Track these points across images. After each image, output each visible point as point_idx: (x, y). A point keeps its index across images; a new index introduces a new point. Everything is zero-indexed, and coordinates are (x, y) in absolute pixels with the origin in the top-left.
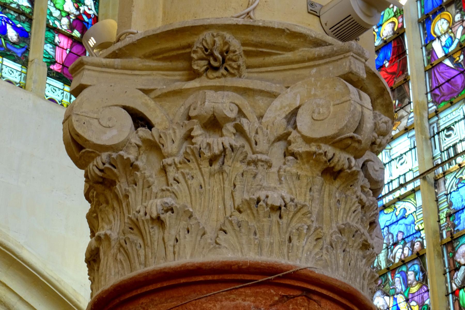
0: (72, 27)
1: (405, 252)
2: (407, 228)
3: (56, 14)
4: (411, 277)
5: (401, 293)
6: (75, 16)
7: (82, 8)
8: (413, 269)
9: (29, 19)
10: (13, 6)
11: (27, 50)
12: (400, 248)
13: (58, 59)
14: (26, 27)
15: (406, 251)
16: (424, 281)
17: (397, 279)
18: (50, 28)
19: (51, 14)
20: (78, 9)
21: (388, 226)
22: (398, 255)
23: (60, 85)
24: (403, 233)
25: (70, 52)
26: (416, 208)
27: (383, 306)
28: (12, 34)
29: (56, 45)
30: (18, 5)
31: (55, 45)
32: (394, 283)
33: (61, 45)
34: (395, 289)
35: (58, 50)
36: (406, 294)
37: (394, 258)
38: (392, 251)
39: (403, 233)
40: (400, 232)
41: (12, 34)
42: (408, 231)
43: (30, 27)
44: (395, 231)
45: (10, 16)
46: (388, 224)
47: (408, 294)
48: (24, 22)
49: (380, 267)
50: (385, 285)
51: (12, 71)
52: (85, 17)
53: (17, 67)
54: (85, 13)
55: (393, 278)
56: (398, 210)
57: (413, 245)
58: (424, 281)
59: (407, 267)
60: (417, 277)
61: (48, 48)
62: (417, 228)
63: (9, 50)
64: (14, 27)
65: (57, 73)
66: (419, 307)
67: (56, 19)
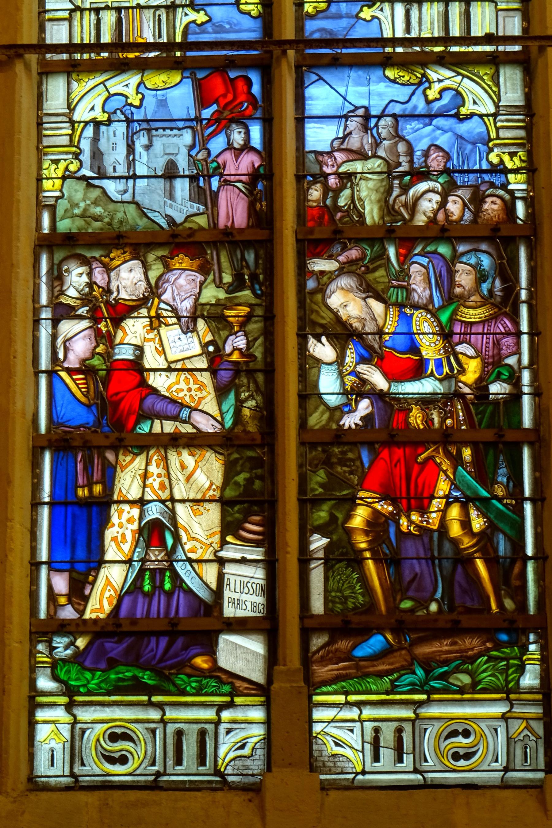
1: (450, 206)
2: (460, 147)
4: (464, 278)
5: (425, 307)
8: (473, 261)
12: (433, 191)
15: (454, 207)
16: (506, 305)
17: (415, 268)
21: (395, 116)
22: (428, 205)
24: (448, 157)
26: (497, 106)
27: (361, 320)
32: (404, 274)
34: (409, 291)
36: (444, 317)
37: (413, 208)
38: (405, 189)
39: (448, 157)
40: (439, 148)
42: (466, 158)
44: (420, 139)
46: (397, 109)
47: (452, 320)
49: (361, 216)
50: (375, 270)
55: (405, 259)
56: (437, 87)
57: (477, 199)
58: (506, 305)
59: (455, 250)
60: (485, 287)
62: (494, 158)
66: (485, 364)
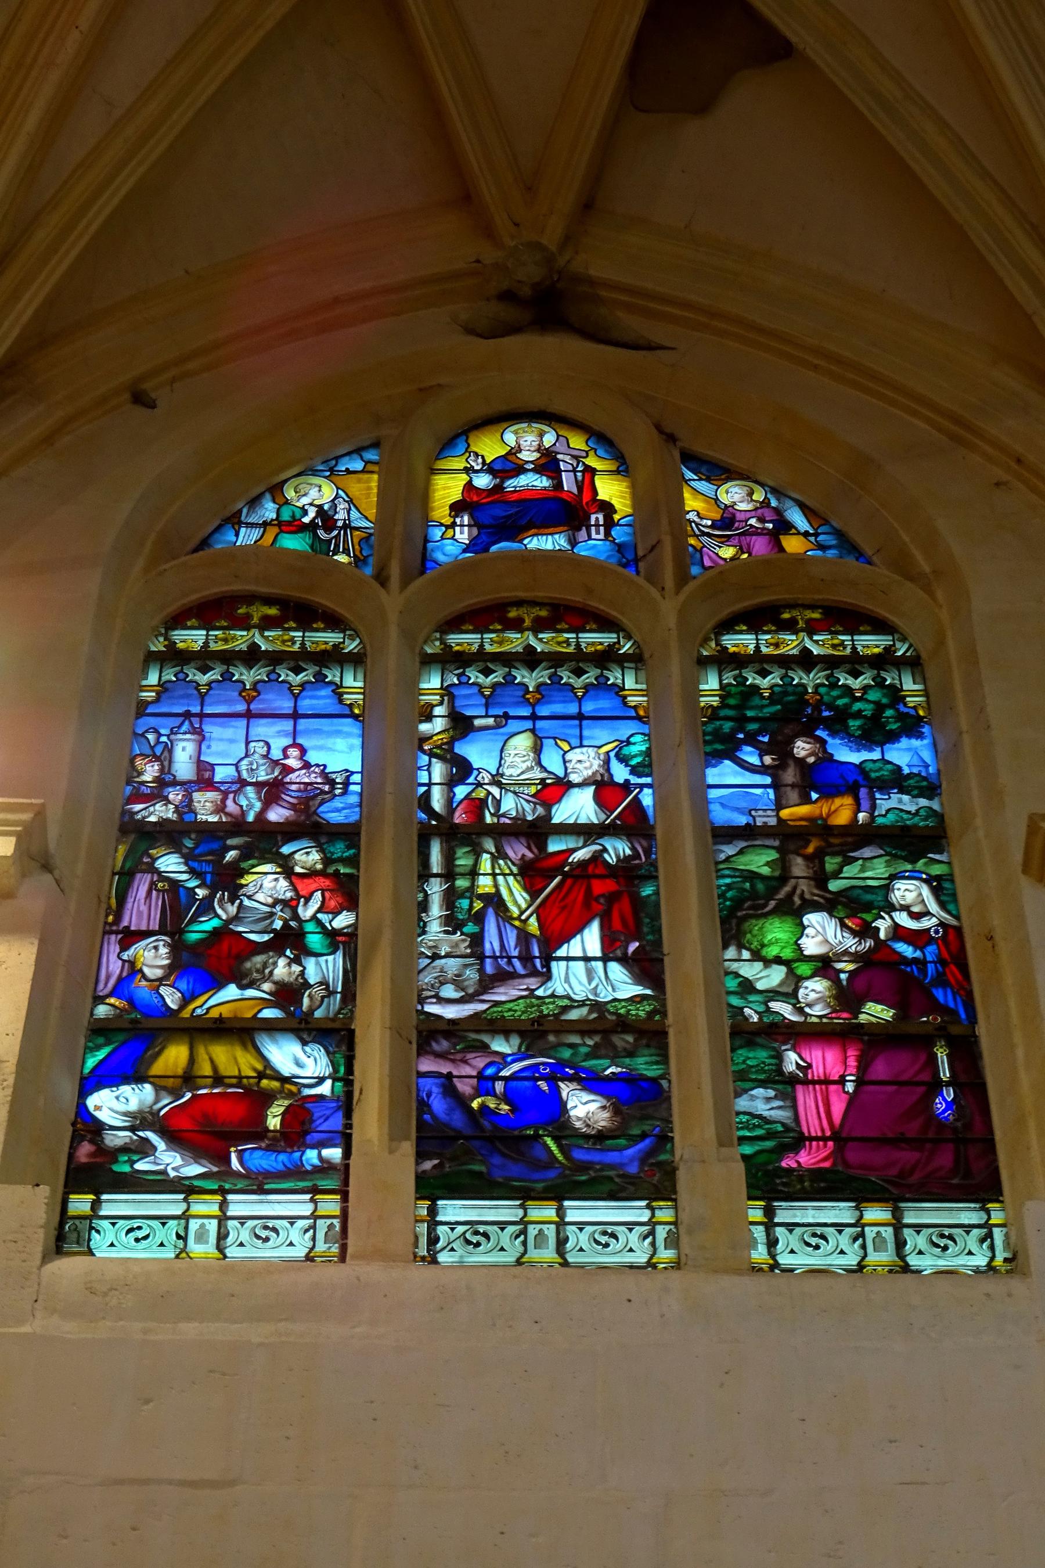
0: (848, 998)
3: (774, 977)
6: (856, 957)
7: (883, 926)
9: (650, 1033)
10: (574, 1015)
11: (664, 1139)
13: (812, 1124)
14: (644, 1066)
18: (744, 1034)
19: (747, 987)
20: (865, 931)
23: (841, 1212)
25: (859, 1083)
28: (583, 1107)
29: (792, 1081)
30: (597, 1006)
31: (787, 1085)
33: (818, 1071)
35: (807, 1099)
41: (583, 1107)
43: (664, 1058)
45: (566, 1054)
48: (631, 1054)
51: (609, 1232)
52: (906, 950)
53: (636, 1211)
54: (899, 932)
61: (760, 1102)
63: (584, 1167)
64: (592, 1083)
65: (816, 1174)
67: (774, 994)
